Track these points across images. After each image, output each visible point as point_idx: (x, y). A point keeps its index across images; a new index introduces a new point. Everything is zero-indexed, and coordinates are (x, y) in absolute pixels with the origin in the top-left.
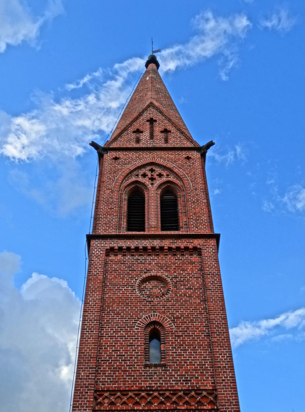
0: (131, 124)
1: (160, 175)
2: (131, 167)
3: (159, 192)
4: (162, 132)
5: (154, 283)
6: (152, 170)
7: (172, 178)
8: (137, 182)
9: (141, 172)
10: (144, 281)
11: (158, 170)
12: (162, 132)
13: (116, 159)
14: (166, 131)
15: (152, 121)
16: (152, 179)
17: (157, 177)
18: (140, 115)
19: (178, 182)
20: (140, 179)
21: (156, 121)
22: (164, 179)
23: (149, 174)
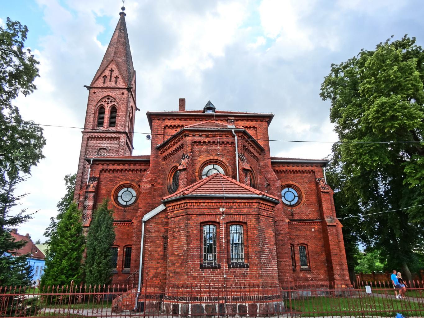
0: (101, 74)
1: (111, 101)
2: (101, 96)
3: (110, 109)
4: (115, 77)
5: (102, 151)
6: (108, 99)
7: (115, 104)
8: (102, 104)
9: (104, 100)
10: (99, 150)
11: (111, 99)
12: (115, 77)
13: (95, 93)
14: (117, 77)
15: (112, 71)
16: (108, 104)
17: (110, 103)
18: (107, 66)
19: (117, 105)
20: (103, 103)
21: (113, 71)
22: (113, 103)
23: (107, 100)
